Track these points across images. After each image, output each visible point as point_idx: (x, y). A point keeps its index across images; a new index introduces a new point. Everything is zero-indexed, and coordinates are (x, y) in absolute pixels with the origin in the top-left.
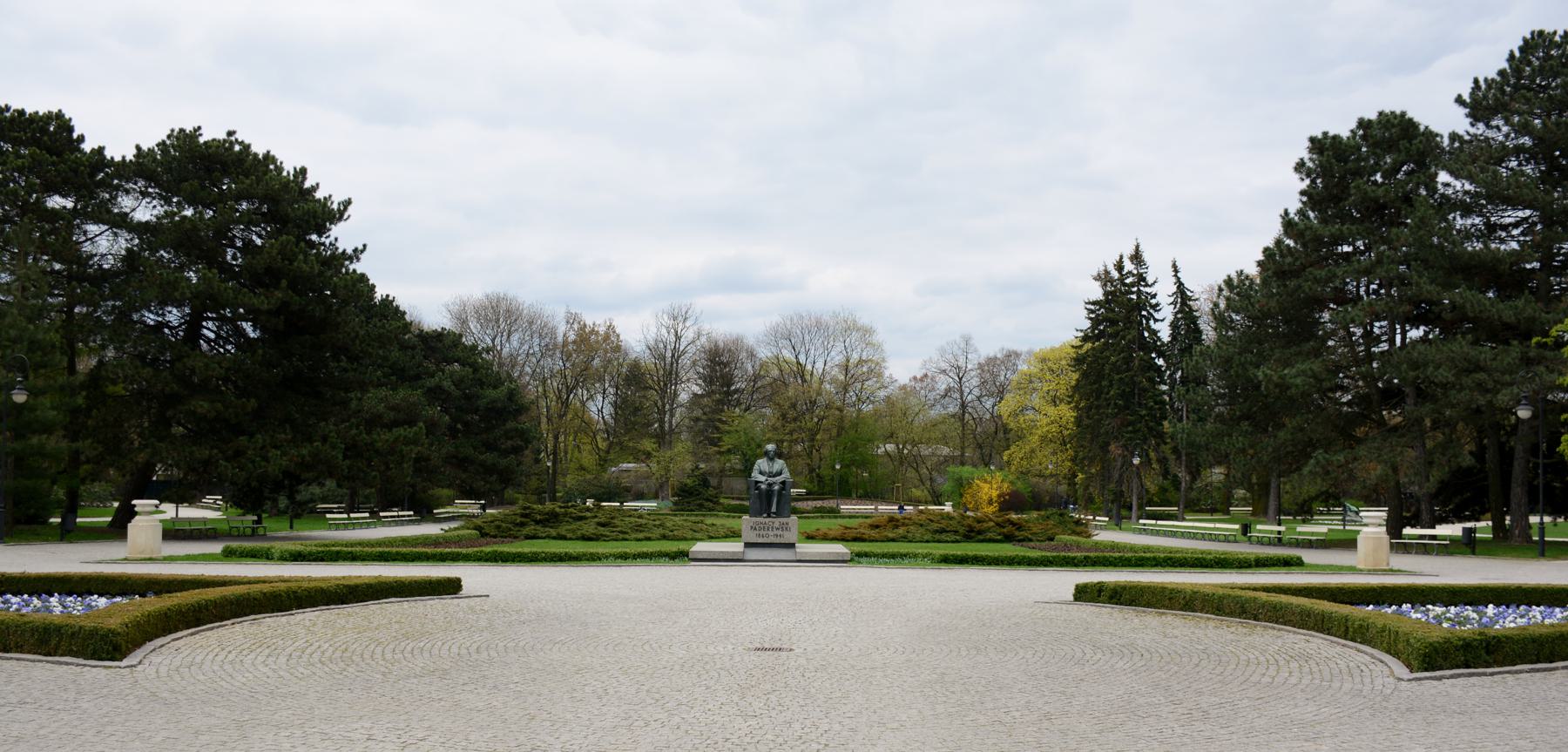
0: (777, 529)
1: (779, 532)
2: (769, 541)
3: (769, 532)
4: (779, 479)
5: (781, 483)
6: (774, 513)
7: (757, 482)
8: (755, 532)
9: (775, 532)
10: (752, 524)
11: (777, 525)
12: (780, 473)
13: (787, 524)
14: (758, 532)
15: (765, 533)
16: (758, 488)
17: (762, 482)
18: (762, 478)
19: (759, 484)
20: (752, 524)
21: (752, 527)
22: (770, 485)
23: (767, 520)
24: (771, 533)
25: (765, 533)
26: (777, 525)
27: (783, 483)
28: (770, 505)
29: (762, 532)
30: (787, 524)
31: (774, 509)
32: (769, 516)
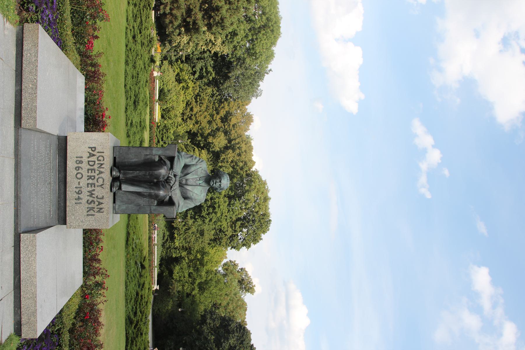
0: (91, 194)
1: (85, 197)
2: (69, 179)
3: (85, 178)
4: (176, 194)
5: (171, 198)
6: (120, 188)
7: (172, 159)
8: (85, 155)
9: (85, 190)
10: (99, 149)
11: (98, 192)
12: (185, 197)
13: (100, 210)
14: (85, 159)
15: (84, 172)
16: (161, 163)
17: (172, 168)
18: (178, 168)
19: (168, 163)
20: (99, 149)
21: (93, 149)
22: (167, 180)
23: (107, 178)
24: (84, 182)
25: (84, 172)
26: (98, 192)
27: (171, 202)
28: (132, 182)
29: (85, 166)
30: (100, 210)
31: (125, 187)
32: (115, 179)
